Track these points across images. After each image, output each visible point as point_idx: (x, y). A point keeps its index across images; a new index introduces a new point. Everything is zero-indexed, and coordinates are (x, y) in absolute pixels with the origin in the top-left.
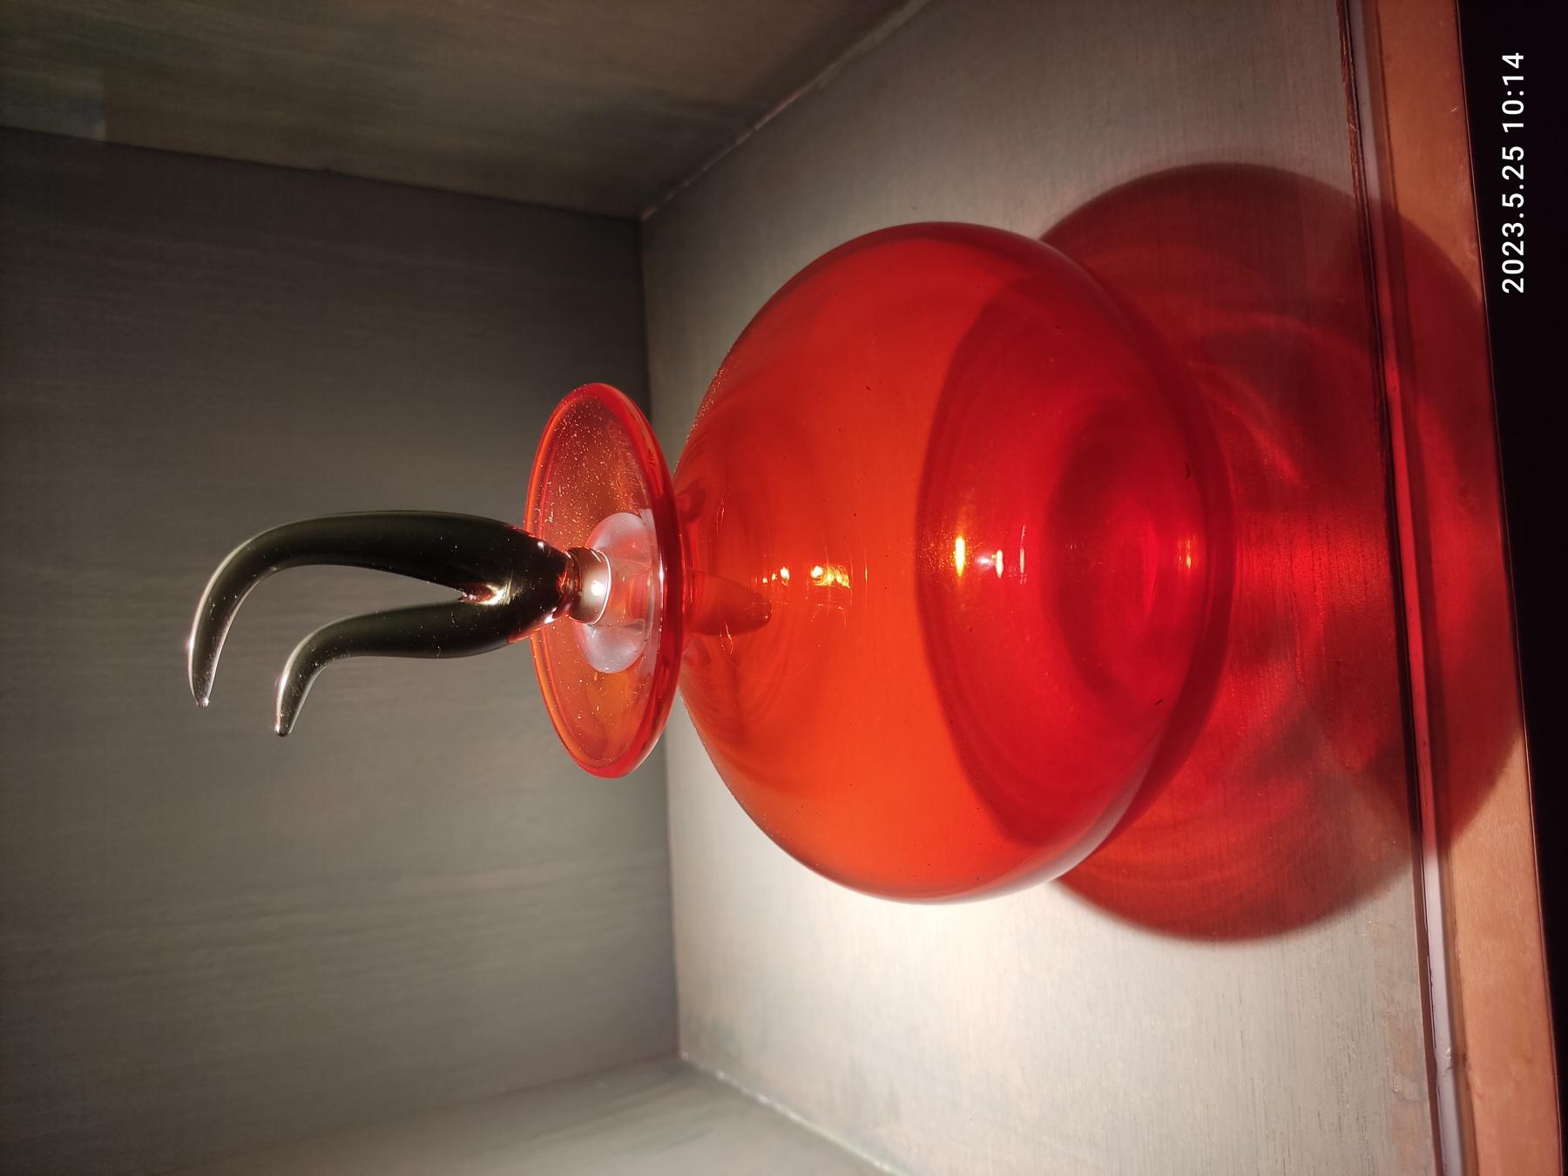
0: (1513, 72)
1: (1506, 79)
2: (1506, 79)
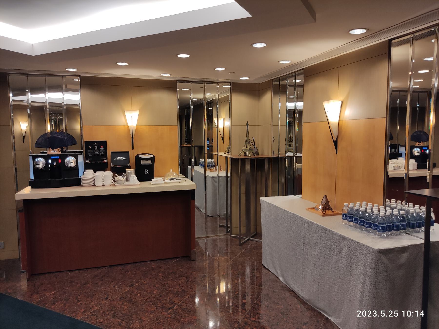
0: (419, 314)
1: (417, 312)
2: (417, 312)
